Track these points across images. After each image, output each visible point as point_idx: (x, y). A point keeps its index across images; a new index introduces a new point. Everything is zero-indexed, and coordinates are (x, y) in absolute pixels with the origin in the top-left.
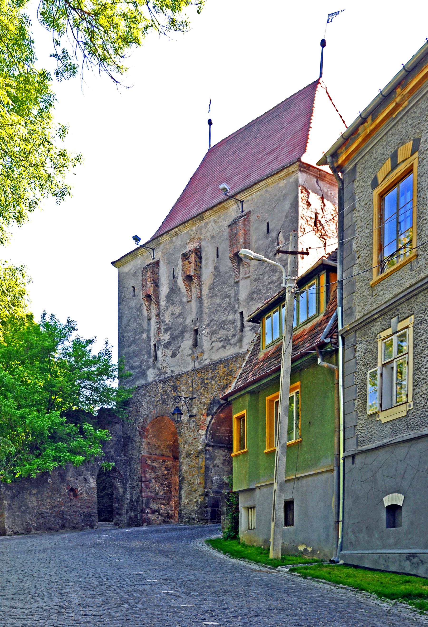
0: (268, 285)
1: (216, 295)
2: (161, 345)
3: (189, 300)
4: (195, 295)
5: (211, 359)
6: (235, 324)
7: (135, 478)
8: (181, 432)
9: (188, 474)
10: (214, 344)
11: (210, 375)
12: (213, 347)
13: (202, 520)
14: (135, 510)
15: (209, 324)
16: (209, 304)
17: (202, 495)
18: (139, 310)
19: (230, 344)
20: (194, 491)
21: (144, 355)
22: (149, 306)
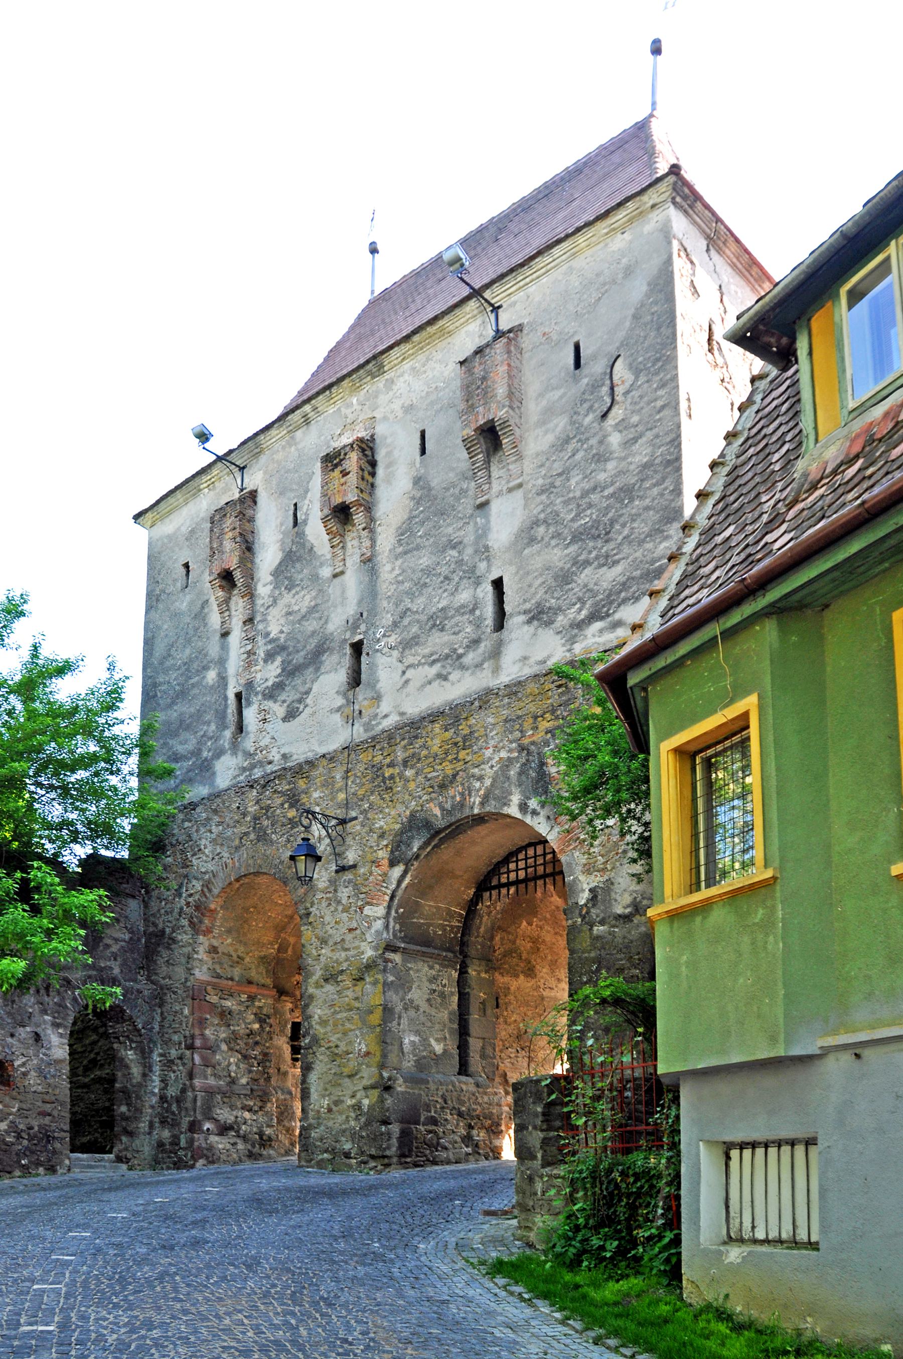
0: (582, 497)
1: (418, 548)
2: (257, 694)
3: (338, 570)
4: (357, 558)
5: (402, 714)
6: (478, 613)
7: (176, 1038)
8: (308, 914)
9: (329, 1028)
10: (410, 673)
11: (400, 755)
12: (407, 682)
13: (373, 1157)
14: (175, 1124)
15: (395, 624)
16: (397, 572)
17: (373, 1087)
18: (200, 615)
19: (463, 668)
20: (349, 1076)
21: (208, 723)
22: (227, 601)
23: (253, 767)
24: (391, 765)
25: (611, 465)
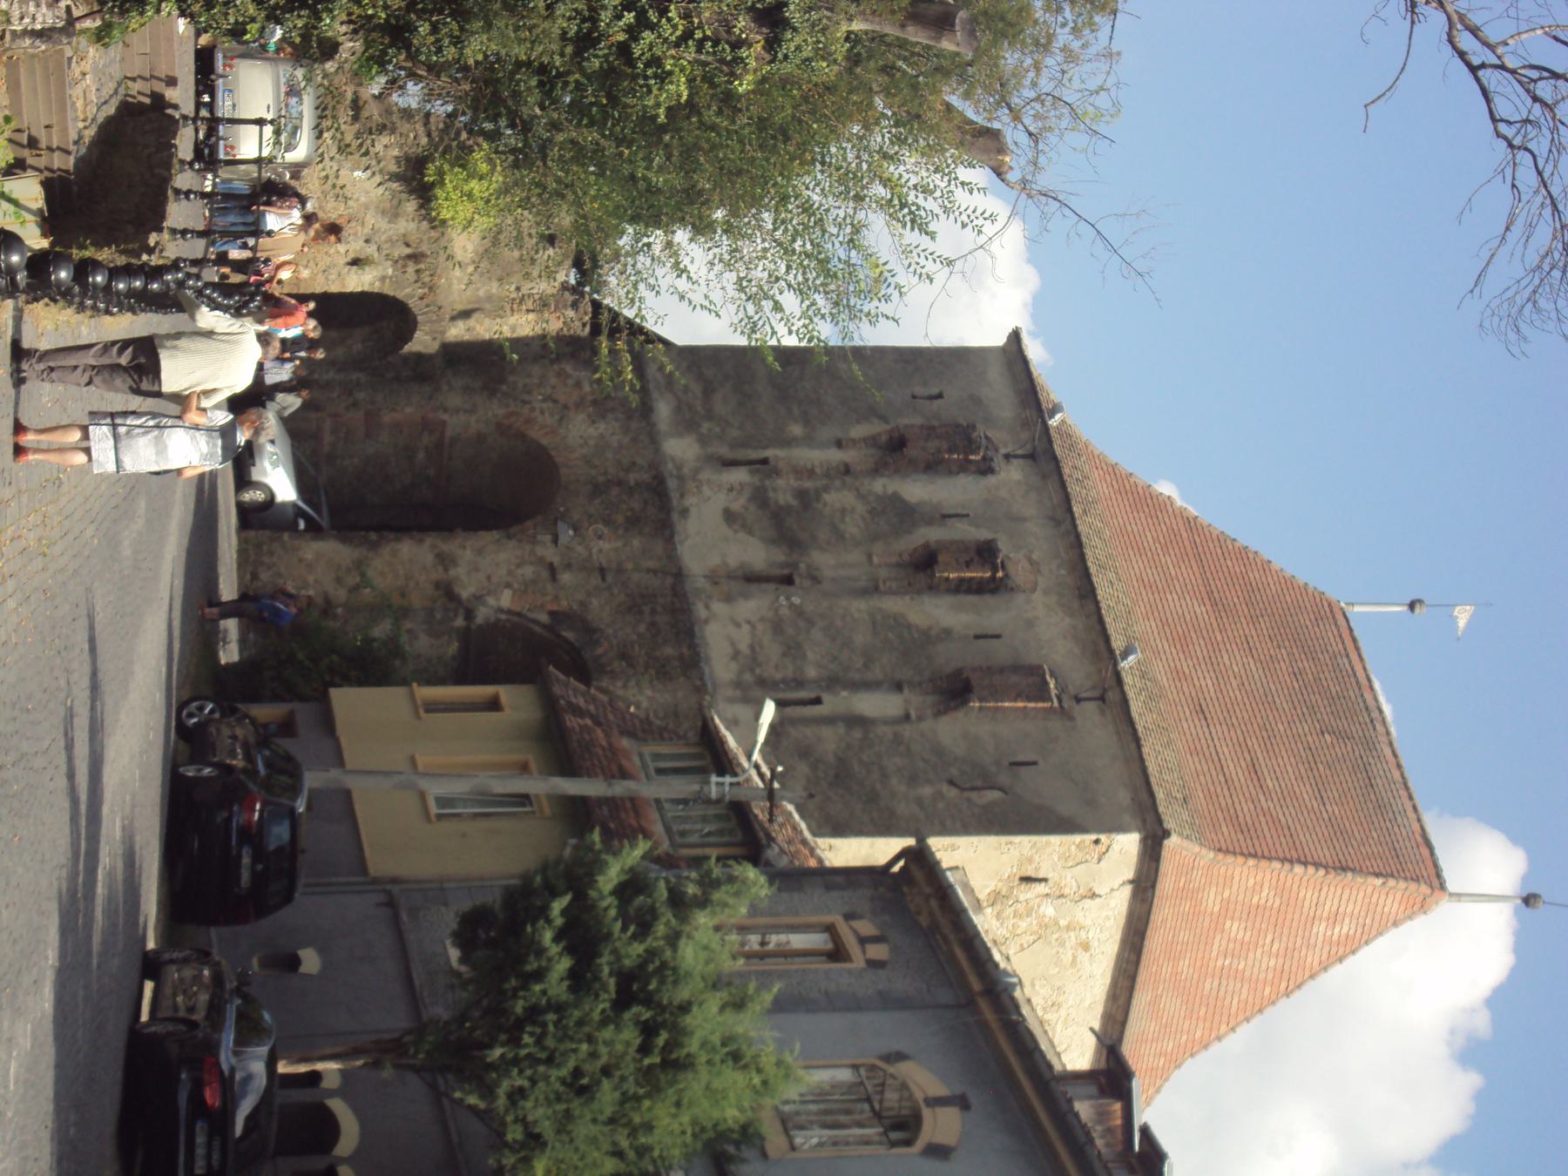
5: (707, 621)
16: (856, 615)
23: (681, 478)
24: (653, 612)
25: (903, 788)
